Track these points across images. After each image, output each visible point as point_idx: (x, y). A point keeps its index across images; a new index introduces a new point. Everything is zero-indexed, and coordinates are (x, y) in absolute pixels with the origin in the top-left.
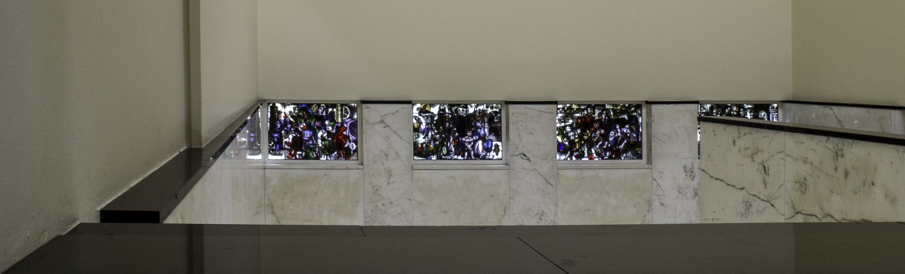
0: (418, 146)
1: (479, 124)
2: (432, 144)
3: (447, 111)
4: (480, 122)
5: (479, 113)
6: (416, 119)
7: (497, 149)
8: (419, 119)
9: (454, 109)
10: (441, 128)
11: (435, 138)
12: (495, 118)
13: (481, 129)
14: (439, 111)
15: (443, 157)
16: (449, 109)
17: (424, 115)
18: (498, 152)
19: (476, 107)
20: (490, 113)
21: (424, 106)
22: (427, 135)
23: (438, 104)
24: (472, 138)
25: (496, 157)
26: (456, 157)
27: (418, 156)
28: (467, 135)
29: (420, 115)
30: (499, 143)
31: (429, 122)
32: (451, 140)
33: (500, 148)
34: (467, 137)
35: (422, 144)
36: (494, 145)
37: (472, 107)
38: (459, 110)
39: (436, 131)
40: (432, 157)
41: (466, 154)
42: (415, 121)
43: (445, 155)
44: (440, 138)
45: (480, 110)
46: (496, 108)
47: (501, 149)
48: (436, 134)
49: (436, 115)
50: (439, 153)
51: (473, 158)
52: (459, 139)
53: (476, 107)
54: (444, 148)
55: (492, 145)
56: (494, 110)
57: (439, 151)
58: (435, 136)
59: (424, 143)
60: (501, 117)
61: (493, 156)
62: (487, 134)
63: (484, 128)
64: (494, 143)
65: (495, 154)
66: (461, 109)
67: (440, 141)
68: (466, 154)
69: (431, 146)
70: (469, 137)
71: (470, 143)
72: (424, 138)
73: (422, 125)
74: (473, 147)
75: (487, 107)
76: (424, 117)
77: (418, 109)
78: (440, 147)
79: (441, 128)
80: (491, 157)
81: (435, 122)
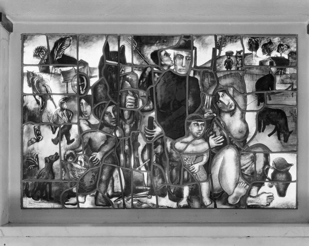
0: (38, 166)
1: (226, 99)
2: (81, 158)
3: (128, 56)
4: (231, 91)
5: (229, 65)
6: (31, 84)
7: (281, 177)
8: (41, 80)
9: (148, 51)
10: (110, 109)
11: (90, 140)
12: (278, 78)
13: (232, 113)
14: (102, 60)
15: (113, 200)
16: (134, 52)
17: (58, 70)
18: (286, 186)
19: (219, 46)
20: (262, 63)
21: (56, 44)
22: (66, 132)
23: (98, 36)
24: (207, 140)
25: (278, 201)
26: (153, 200)
27: (36, 198)
28: (190, 133)
29: (46, 71)
30: (290, 158)
31: (71, 91)
32: (140, 148)
33: (293, 171)
34: (189, 139)
35: (50, 161)
36: (271, 164)
37: (204, 45)
38: (167, 54)
39: (94, 121)
40: (81, 199)
41: (186, 191)
42: (27, 89)
43: (120, 195)
44: (106, 143)
45: (229, 54)
46: (280, 48)
47: (294, 178)
48: (93, 128)
49: (94, 69)
50: (103, 186)
51: (207, 201)
52: (163, 145)
53: (219, 46)
54: (116, 172)
55: (267, 163)
56: (275, 54)
57: (101, 181)
58: (89, 135)
59: (57, 156)
60: (295, 77)
61: (271, 198)
62: (253, 128)
63: (243, 112)
64: (273, 158)
65: (274, 190)
66: (172, 52)
67: (106, 149)
68: (186, 191)
69: (77, 166)
70: (195, 138)
71: (199, 155)
72: (55, 142)
73: (49, 102)
74: (208, 167)
75: (254, 46)
76: (56, 75)
77: (39, 51)
78: (106, 170)
79: (110, 109)
80: (263, 200)
81: (90, 93)
